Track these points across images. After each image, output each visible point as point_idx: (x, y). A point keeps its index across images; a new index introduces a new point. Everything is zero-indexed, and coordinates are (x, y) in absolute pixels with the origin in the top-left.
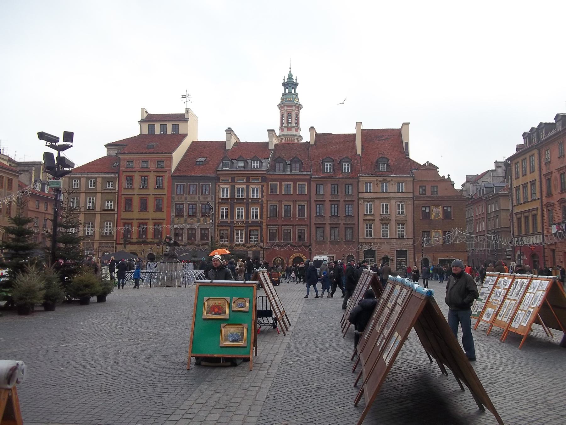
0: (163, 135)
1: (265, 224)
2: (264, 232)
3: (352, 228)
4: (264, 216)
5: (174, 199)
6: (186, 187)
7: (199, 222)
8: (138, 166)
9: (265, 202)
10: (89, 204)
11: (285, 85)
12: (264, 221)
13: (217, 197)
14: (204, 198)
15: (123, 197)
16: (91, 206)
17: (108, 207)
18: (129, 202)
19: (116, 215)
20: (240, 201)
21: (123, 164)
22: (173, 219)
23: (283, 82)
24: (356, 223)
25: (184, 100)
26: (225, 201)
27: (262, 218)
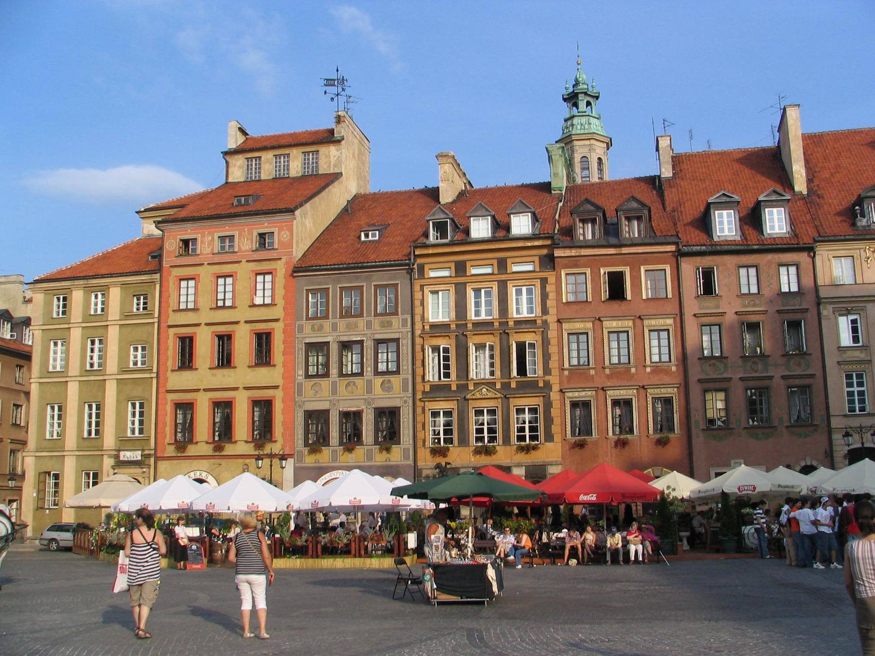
0: (282, 181)
1: (556, 388)
2: (555, 412)
3: (809, 386)
4: (553, 364)
5: (301, 330)
6: (334, 297)
7: (369, 390)
8: (209, 251)
9: (553, 326)
10: (92, 358)
11: (572, 99)
12: (554, 380)
13: (418, 318)
14: (383, 325)
15: (172, 331)
16: (96, 359)
17: (135, 363)
18: (187, 345)
19: (155, 381)
20: (482, 326)
21: (172, 245)
22: (300, 385)
23: (565, 92)
24: (819, 374)
25: (333, 90)
26: (439, 329)
27: (547, 371)
